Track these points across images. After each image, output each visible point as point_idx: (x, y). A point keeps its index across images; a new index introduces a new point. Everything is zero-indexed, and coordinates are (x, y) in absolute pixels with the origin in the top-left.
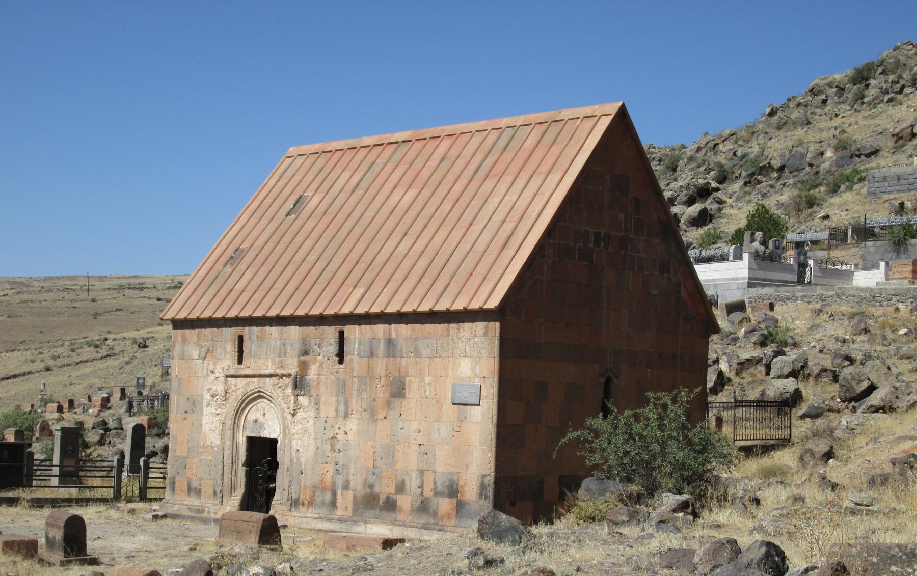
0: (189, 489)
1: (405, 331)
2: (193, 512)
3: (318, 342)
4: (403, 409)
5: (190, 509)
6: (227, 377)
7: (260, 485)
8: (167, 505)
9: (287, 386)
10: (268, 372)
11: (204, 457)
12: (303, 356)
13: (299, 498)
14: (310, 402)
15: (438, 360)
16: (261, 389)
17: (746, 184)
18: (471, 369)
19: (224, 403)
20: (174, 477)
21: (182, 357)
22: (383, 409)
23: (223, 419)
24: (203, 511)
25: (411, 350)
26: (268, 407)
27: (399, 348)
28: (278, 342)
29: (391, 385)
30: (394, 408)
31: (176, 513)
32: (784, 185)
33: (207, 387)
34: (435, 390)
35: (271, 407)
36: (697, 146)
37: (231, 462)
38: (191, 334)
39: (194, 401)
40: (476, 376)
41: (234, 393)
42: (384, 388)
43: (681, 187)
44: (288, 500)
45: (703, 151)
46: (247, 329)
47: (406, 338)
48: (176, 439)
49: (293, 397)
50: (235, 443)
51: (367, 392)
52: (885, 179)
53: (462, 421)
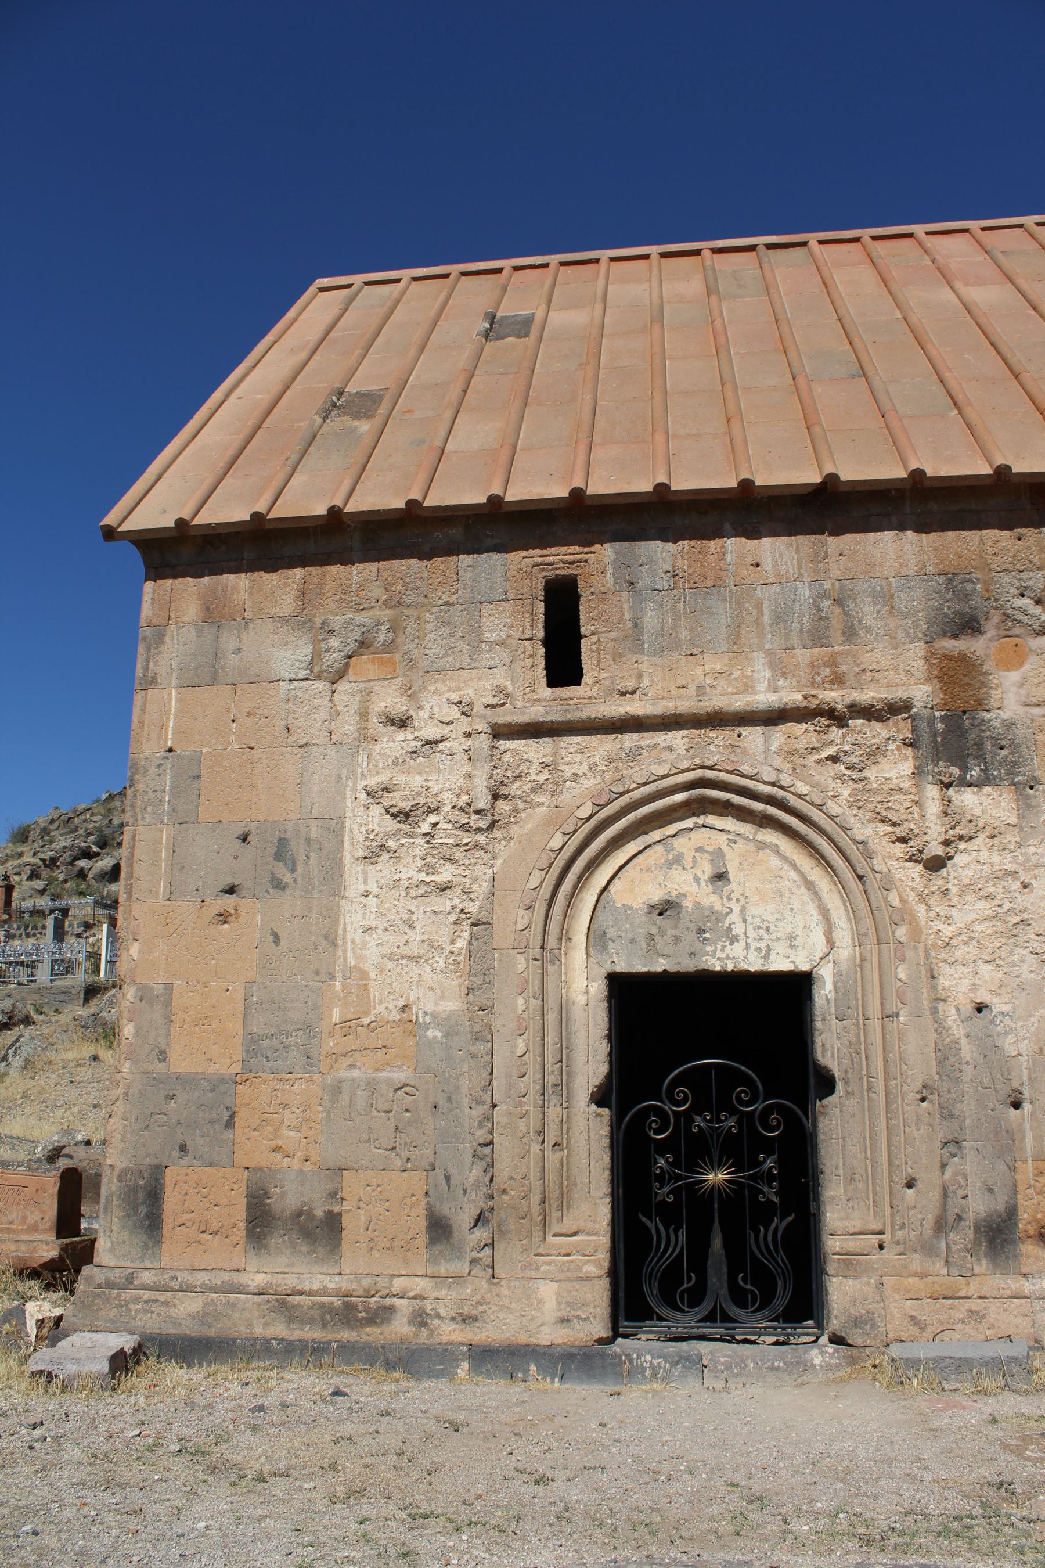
2: (311, 1321)
5: (283, 1304)
7: (661, 1179)
8: (127, 1295)
9: (875, 753)
10: (764, 699)
11: (356, 1073)
12: (955, 636)
13: (1012, 1213)
16: (710, 774)
19: (481, 838)
20: (157, 1172)
23: (472, 908)
24: (381, 1315)
26: (741, 844)
28: (805, 592)
31: (190, 1329)
33: (373, 782)
35: (762, 846)
36: (50, 817)
37: (536, 1087)
39: (283, 842)
41: (542, 799)
43: (65, 847)
44: (941, 1226)
45: (57, 824)
46: (606, 553)
48: (168, 1002)
49: (932, 792)
50: (551, 1003)
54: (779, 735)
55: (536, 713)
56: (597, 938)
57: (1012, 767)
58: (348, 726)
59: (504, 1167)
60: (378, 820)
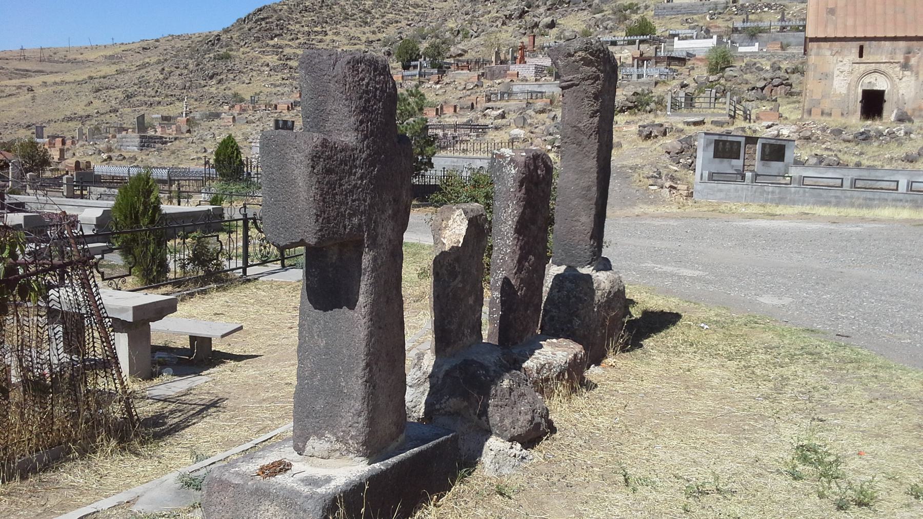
0: (822, 113)
3: (919, 48)
6: (853, 63)
10: (884, 61)
14: (912, 73)
17: (548, 9)
21: (818, 54)
28: (890, 48)
32: (572, 10)
38: (827, 44)
43: (515, 9)
46: (867, 42)
49: (901, 72)
52: (664, 8)
54: (885, 65)
55: (858, 61)
56: (862, 85)
57: (911, 69)
58: (835, 62)
59: (850, 108)
60: (838, 72)
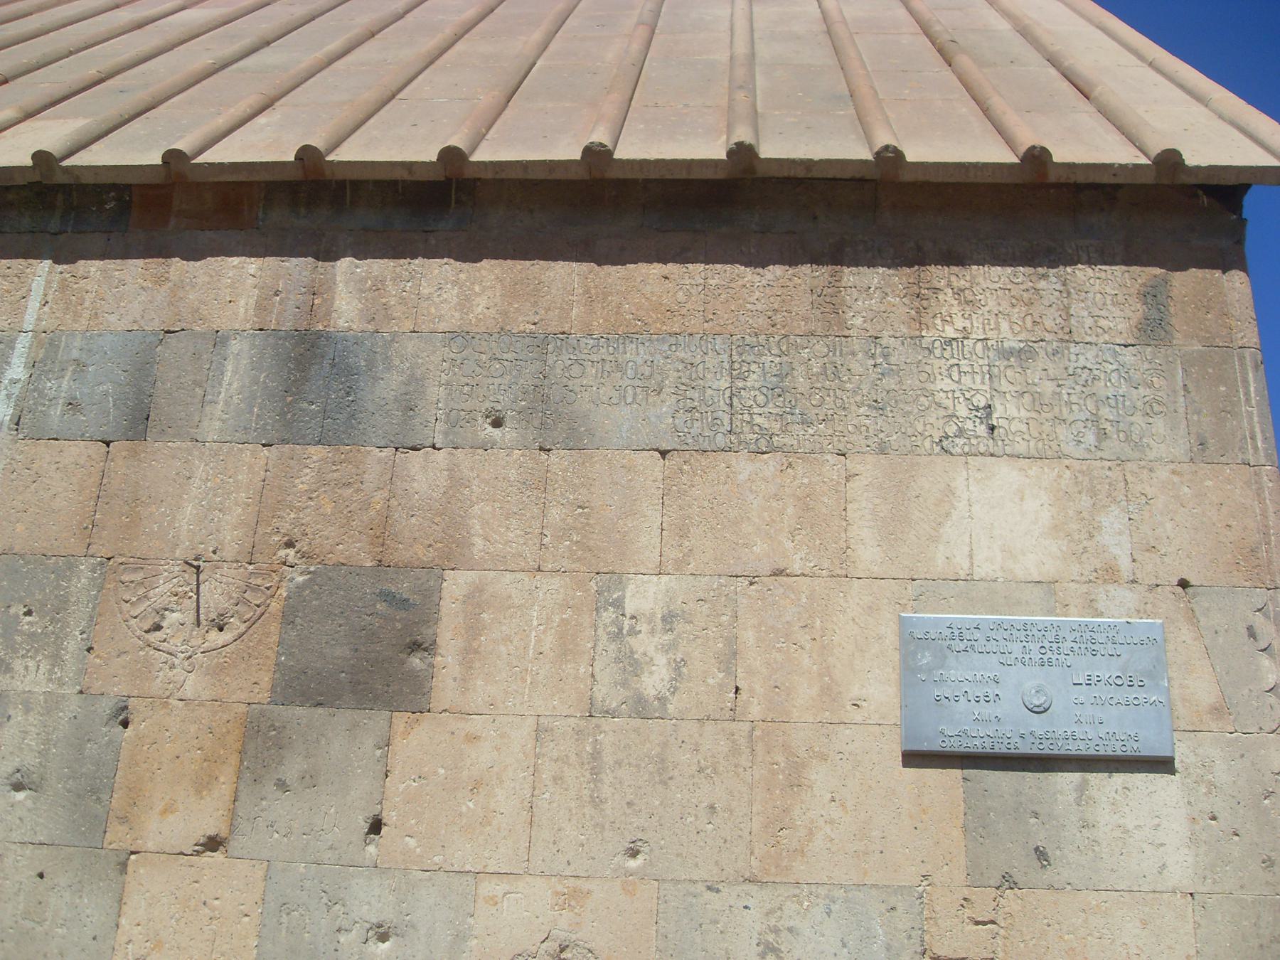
1: (451, 294)
4: (397, 786)
15: (744, 466)
18: (1056, 529)
22: (202, 785)
25: (503, 403)
27: (389, 386)
29: (288, 618)
30: (310, 779)
34: (730, 658)
40: (1110, 574)
42: (216, 638)
47: (452, 335)
51: (56, 659)
53: (1009, 882)
